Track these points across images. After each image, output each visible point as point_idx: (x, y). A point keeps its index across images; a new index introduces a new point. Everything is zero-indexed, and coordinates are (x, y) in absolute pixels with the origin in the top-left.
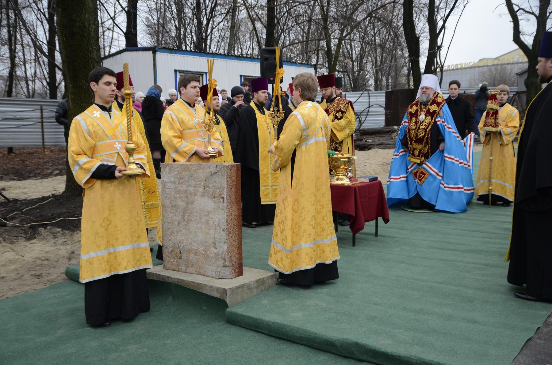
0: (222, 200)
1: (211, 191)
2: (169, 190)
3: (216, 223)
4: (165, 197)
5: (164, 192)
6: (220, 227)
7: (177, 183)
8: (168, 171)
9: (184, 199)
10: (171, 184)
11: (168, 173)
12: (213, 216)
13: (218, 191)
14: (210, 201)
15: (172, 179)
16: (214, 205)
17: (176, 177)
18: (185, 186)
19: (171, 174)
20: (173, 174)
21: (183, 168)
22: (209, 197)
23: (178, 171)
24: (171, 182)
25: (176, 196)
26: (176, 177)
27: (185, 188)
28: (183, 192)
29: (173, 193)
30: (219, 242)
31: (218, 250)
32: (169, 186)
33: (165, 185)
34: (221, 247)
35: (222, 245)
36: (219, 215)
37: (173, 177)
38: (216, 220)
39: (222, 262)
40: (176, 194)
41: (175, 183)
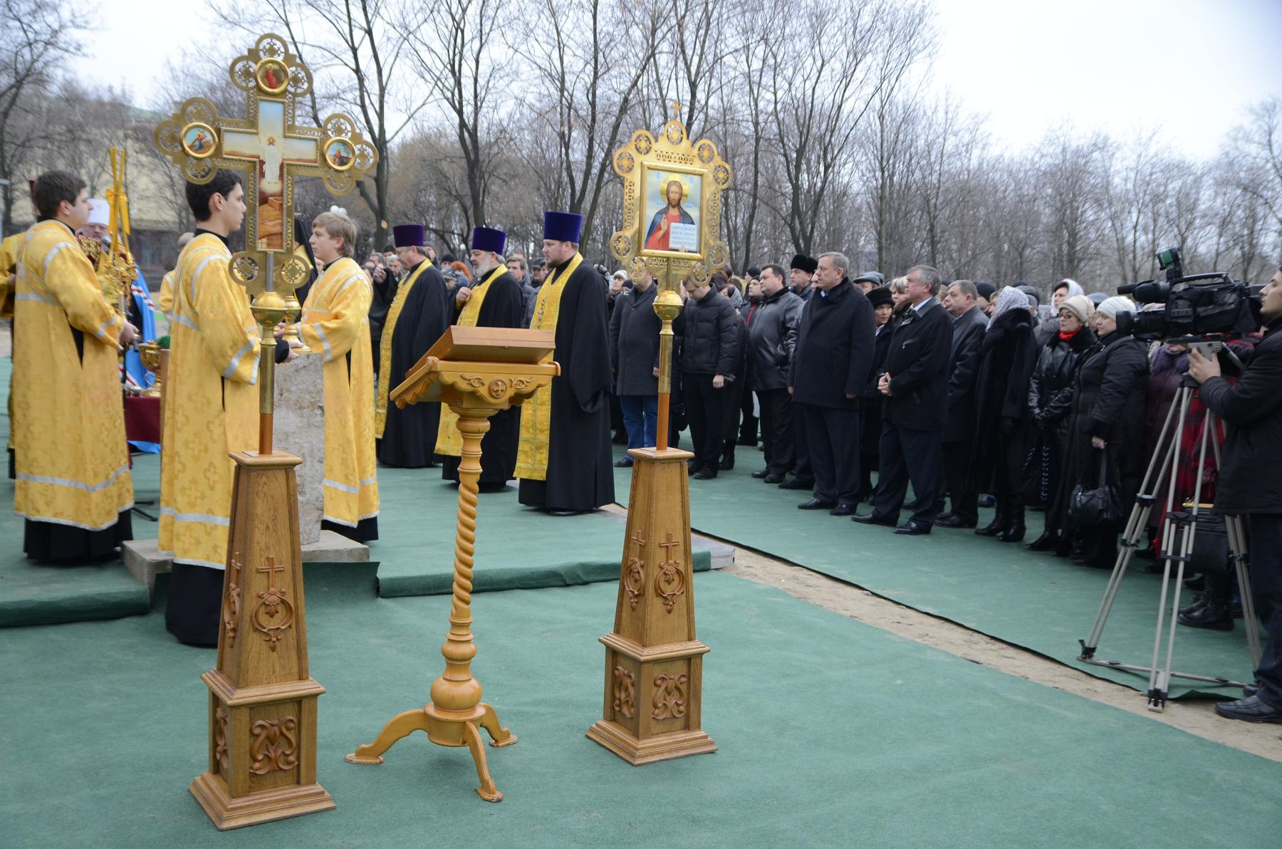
0: (319, 412)
1: (294, 397)
3: (305, 451)
6: (312, 456)
12: (297, 440)
13: (308, 396)
14: (291, 415)
16: (301, 421)
22: (288, 408)
30: (311, 483)
31: (308, 495)
34: (313, 489)
35: (315, 486)
36: (311, 436)
38: (305, 445)
39: (317, 515)
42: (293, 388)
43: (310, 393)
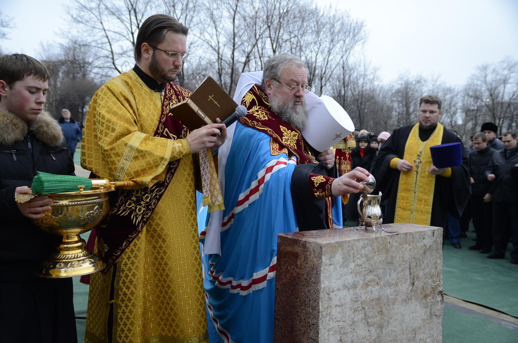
2: (339, 309)
4: (329, 331)
5: (328, 318)
7: (359, 287)
8: (341, 260)
9: (374, 320)
10: (345, 292)
11: (340, 266)
15: (350, 279)
17: (360, 273)
18: (378, 287)
19: (347, 266)
20: (352, 265)
21: (376, 248)
23: (366, 256)
24: (345, 287)
25: (355, 319)
26: (360, 273)
27: (377, 293)
28: (374, 303)
29: (349, 312)
32: (340, 299)
33: (330, 299)
37: (351, 273)
40: (356, 314)
41: (354, 286)
42: (421, 274)
43: (432, 276)
